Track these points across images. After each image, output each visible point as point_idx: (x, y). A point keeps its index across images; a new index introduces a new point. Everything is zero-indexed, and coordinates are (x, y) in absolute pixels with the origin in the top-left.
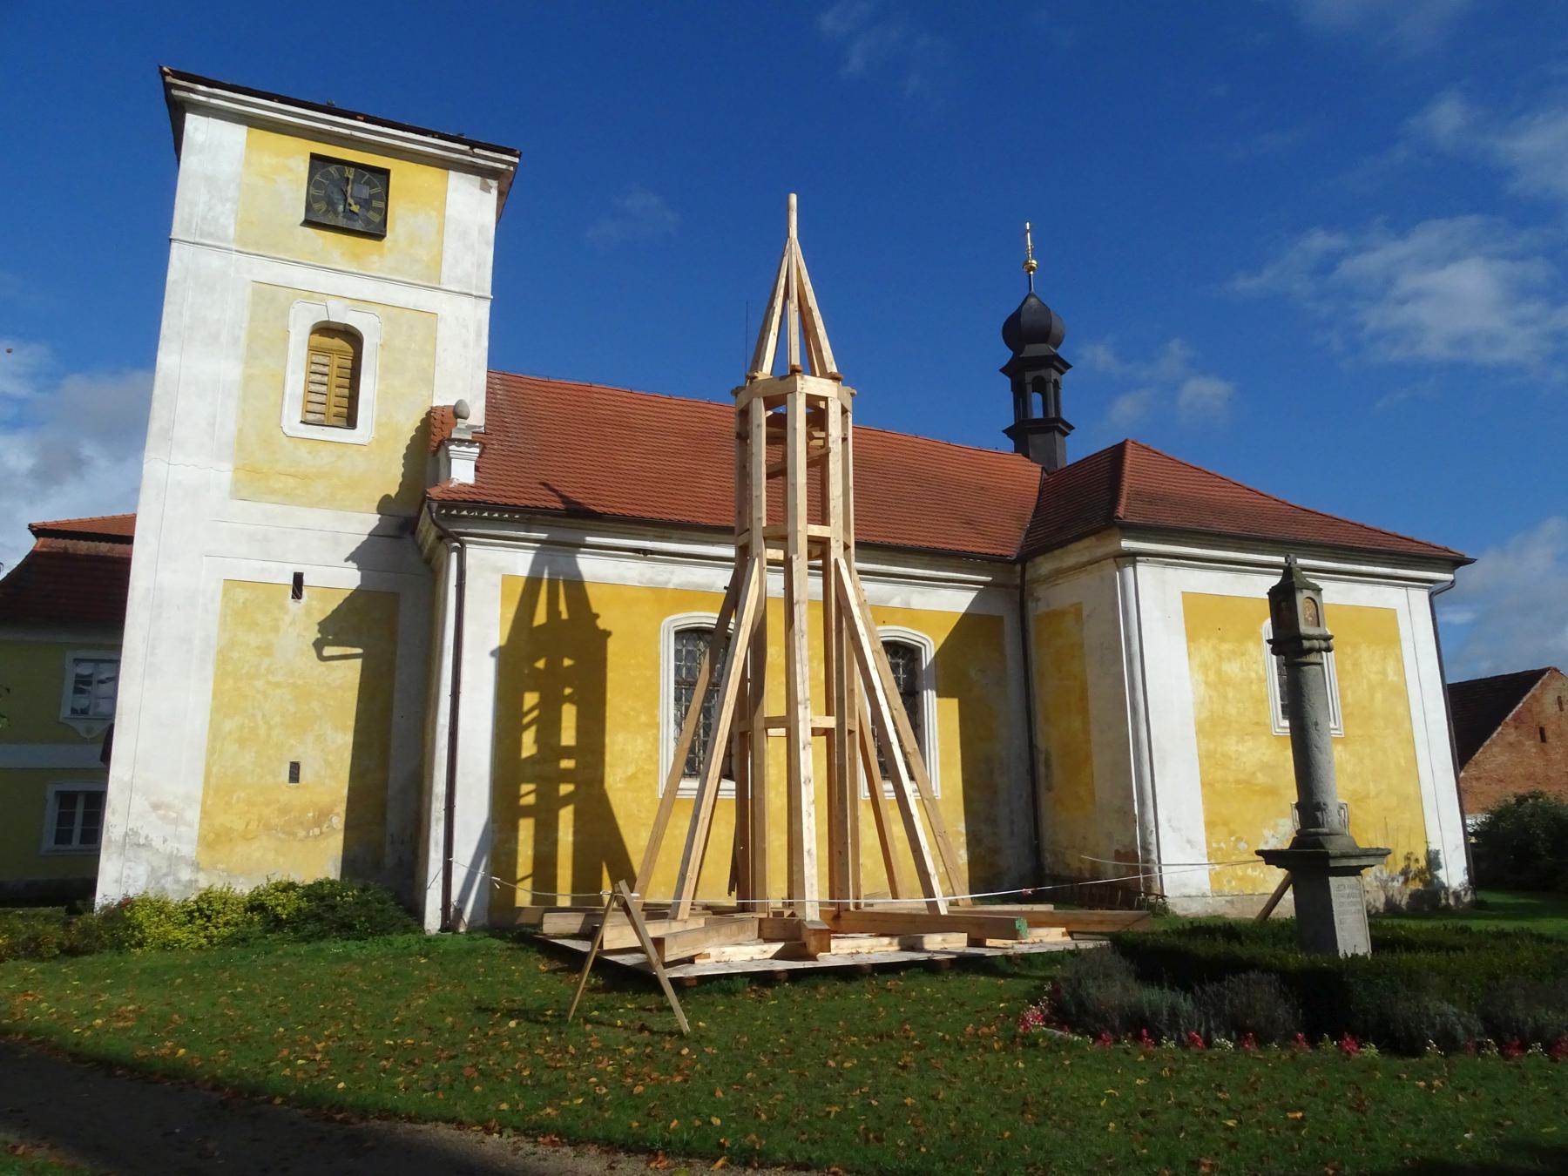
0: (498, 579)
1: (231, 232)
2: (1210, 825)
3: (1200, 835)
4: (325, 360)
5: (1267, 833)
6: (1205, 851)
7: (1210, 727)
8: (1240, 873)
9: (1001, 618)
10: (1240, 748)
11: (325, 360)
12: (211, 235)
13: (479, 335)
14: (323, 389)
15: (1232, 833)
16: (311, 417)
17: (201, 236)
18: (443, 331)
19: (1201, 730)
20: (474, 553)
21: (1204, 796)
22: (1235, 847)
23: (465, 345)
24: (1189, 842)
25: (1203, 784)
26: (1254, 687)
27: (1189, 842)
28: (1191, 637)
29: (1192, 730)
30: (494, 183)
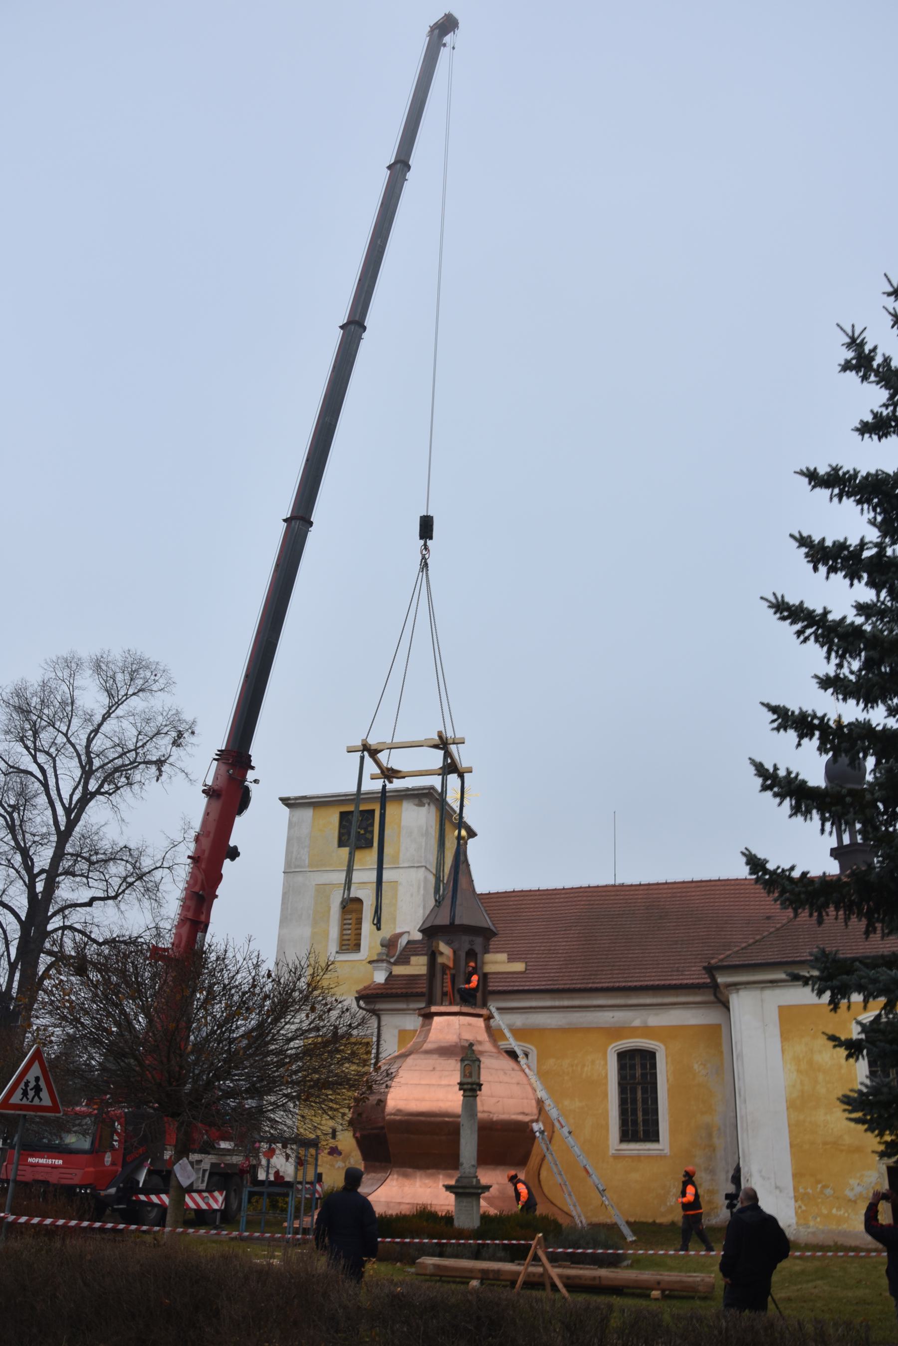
0: (396, 1032)
1: (307, 862)
2: (797, 1176)
3: (788, 1181)
4: (350, 917)
5: (853, 1182)
6: (792, 1194)
7: (799, 1103)
8: (825, 1211)
9: (719, 1026)
10: (828, 1117)
11: (350, 917)
12: (299, 866)
13: (419, 888)
14: (349, 932)
15: (818, 1182)
16: (344, 947)
17: (295, 867)
18: (401, 890)
19: (792, 1105)
20: (386, 1019)
21: (793, 1155)
22: (822, 1192)
23: (412, 895)
24: (777, 1187)
25: (791, 1146)
26: (843, 1071)
27: (777, 1187)
28: (785, 1036)
29: (783, 1106)
30: (425, 801)
